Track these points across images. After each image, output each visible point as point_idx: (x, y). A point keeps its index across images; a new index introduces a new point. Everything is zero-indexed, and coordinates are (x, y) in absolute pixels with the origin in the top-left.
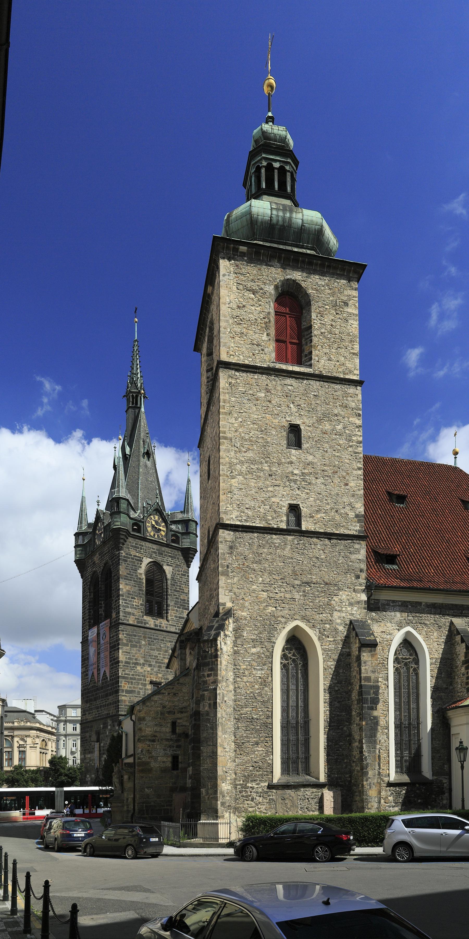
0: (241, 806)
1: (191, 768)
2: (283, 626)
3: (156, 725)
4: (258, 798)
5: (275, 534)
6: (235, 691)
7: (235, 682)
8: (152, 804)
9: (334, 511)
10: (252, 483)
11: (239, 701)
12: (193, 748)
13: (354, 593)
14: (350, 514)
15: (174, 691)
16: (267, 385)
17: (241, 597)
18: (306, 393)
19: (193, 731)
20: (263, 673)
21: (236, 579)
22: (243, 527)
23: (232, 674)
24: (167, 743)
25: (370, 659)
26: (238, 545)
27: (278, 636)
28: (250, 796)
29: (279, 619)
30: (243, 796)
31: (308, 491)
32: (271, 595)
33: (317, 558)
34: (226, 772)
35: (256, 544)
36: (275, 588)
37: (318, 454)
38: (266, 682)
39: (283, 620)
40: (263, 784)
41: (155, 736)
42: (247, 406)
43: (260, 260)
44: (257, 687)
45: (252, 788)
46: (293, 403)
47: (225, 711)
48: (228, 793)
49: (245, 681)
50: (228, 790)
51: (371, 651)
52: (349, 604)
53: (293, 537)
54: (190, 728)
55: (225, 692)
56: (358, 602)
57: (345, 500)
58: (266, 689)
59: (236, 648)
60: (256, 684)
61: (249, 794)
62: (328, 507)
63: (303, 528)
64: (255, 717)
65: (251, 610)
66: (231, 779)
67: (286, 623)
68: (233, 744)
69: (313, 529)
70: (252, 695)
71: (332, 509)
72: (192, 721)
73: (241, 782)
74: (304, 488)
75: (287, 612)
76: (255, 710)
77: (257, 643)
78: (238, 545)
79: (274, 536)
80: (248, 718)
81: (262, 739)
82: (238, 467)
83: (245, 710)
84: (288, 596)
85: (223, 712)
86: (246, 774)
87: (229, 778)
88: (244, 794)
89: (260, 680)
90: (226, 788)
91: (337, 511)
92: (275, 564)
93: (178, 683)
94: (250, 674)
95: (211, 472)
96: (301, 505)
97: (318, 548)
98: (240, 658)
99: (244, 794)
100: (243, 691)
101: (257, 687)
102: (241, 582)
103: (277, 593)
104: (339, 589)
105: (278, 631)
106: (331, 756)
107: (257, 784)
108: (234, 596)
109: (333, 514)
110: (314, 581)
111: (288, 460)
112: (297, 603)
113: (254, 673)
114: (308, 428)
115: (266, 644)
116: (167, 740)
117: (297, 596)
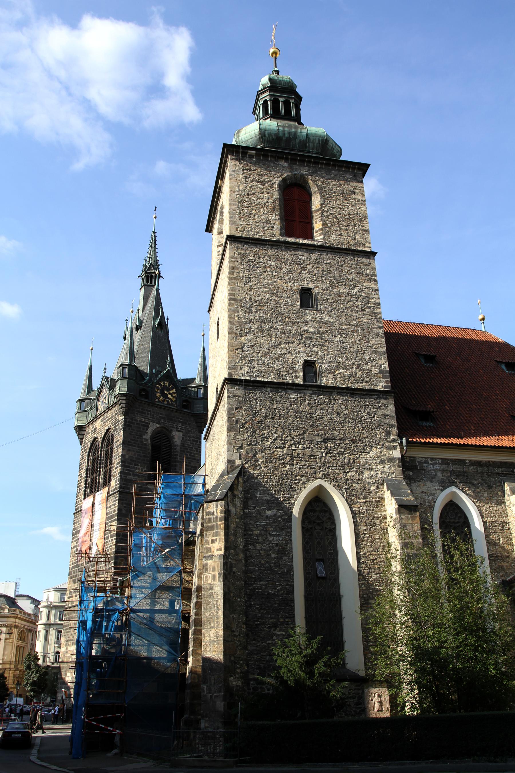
6: (246, 561)
7: (246, 550)
11: (251, 573)
20: (281, 539)
23: (242, 540)
25: (410, 522)
31: (326, 348)
34: (235, 663)
38: (285, 550)
43: (268, 160)
44: (273, 555)
47: (233, 584)
49: (258, 548)
50: (237, 686)
58: (284, 558)
60: (273, 553)
66: (241, 673)
68: (244, 626)
76: (272, 584)
77: (273, 505)
83: (259, 584)
84: (308, 452)
86: (262, 665)
89: (277, 548)
90: (234, 683)
94: (264, 540)
98: (253, 522)
105: (298, 491)
114: (321, 291)
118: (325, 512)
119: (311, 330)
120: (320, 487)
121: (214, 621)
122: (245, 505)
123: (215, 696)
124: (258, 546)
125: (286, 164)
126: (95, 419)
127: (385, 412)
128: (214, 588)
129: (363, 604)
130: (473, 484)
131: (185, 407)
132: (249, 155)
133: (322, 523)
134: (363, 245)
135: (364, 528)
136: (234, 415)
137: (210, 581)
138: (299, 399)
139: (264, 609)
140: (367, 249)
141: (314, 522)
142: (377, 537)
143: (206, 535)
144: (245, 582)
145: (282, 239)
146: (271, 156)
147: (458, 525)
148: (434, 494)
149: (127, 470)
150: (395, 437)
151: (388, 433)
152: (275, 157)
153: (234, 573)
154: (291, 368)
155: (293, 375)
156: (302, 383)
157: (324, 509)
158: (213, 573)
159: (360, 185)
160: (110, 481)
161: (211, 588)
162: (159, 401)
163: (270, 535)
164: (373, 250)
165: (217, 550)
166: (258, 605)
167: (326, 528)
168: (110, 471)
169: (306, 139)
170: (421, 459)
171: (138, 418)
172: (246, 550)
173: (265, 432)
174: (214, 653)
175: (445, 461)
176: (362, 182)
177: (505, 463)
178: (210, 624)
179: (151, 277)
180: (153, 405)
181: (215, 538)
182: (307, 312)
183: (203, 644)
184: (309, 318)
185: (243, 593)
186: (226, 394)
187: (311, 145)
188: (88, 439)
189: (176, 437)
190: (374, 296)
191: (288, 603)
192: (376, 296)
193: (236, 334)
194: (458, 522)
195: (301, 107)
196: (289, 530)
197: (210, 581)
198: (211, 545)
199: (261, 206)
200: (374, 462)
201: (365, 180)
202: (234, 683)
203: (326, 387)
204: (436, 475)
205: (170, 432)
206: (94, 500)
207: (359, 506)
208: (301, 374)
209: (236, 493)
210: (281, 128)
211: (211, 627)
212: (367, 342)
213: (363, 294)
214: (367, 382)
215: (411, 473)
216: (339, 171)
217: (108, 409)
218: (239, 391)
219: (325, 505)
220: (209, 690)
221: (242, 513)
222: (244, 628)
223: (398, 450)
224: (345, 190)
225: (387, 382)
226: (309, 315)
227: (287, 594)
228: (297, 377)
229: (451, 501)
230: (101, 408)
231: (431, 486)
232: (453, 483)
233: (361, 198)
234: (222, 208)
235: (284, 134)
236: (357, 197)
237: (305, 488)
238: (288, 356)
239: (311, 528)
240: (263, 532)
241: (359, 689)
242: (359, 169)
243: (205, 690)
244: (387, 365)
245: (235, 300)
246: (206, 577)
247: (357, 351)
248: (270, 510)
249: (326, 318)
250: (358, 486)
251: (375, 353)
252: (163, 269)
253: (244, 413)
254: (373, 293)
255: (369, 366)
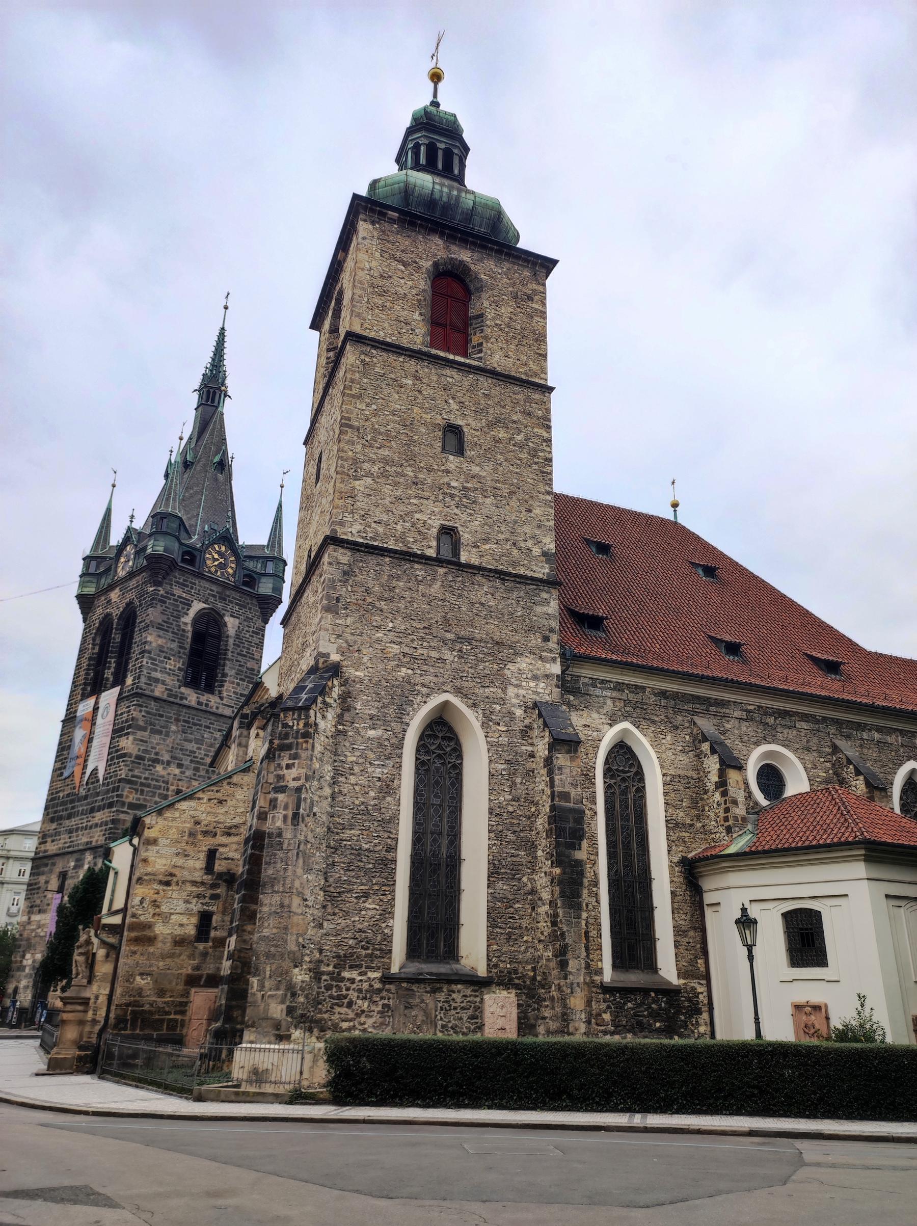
0: (326, 1016)
1: (233, 939)
2: (424, 699)
3: (177, 854)
4: (360, 1002)
5: (418, 563)
6: (333, 799)
7: (334, 783)
8: (146, 1007)
9: (509, 543)
10: (387, 490)
11: (339, 816)
12: (243, 900)
13: (540, 662)
14: (534, 549)
15: (219, 795)
16: (417, 371)
17: (356, 648)
18: (472, 389)
19: (247, 867)
20: (386, 771)
21: (349, 621)
22: (367, 546)
23: (330, 768)
24: (194, 889)
26: (357, 570)
27: (414, 715)
28: (345, 997)
29: (417, 688)
30: (331, 997)
32: (406, 650)
33: (481, 604)
34: (304, 947)
35: (387, 573)
36: (413, 641)
37: (488, 467)
38: (388, 788)
39: (425, 690)
40: (372, 975)
41: (172, 875)
42: (385, 392)
44: (372, 794)
45: (352, 981)
46: (453, 398)
47: (312, 831)
48: (302, 989)
49: (352, 782)
50: (303, 982)
51: (569, 752)
52: (533, 676)
53: (446, 570)
54: (241, 863)
55: (316, 798)
56: (547, 676)
57: (527, 531)
58: (389, 799)
59: (341, 727)
61: (344, 992)
62: (502, 537)
63: (463, 559)
64: (367, 846)
65: (371, 670)
66: (310, 962)
67: (428, 695)
68: (322, 893)
69: (477, 563)
70: (363, 807)
71: (507, 540)
72: (246, 850)
73: (331, 968)
74: (466, 507)
75: (431, 678)
77: (378, 722)
78: (357, 570)
79: (417, 566)
80: (352, 849)
81: (376, 887)
82: (366, 466)
84: (434, 654)
85: (309, 833)
86: (342, 953)
87: (307, 959)
88: (334, 992)
89: (379, 784)
90: (300, 977)
91: (514, 544)
92: (415, 605)
93: (229, 783)
95: (322, 472)
96: (460, 529)
97: (484, 592)
98: (347, 744)
99: (334, 992)
100: (348, 800)
101: (372, 794)
102: (358, 625)
103: (415, 648)
104: (515, 653)
105: (415, 706)
106: (500, 928)
107: (361, 974)
108: (344, 645)
109: (509, 547)
110: (478, 636)
111: (443, 468)
112: (448, 667)
113: (370, 770)
115: (393, 724)
116: (194, 883)
117: (448, 656)
118: (450, 739)
119: (454, 484)
120: (446, 704)
121: (279, 882)
122: (340, 719)
123: (270, 996)
124: (353, 779)
125: (440, 242)
126: (111, 588)
127: (545, 609)
128: (284, 834)
129: (492, 873)
130: (654, 722)
131: (245, 584)
132: (389, 218)
133: (445, 754)
134: (536, 375)
135: (503, 767)
136: (335, 589)
137: (279, 823)
138: (429, 578)
139: (353, 870)
140: (541, 382)
141: (434, 753)
142: (518, 780)
143: (279, 756)
144: (329, 829)
145: (426, 349)
146: (421, 226)
147: (628, 774)
148: (598, 730)
149: (152, 664)
150: (555, 646)
151: (546, 639)
152: (425, 228)
153: (315, 814)
154: (420, 533)
155: (423, 544)
156: (434, 556)
157: (448, 735)
158: (284, 812)
159: (541, 288)
160: (125, 676)
161: (280, 835)
162: (210, 572)
163: (370, 763)
164: (550, 384)
165: (294, 779)
166: (344, 863)
167: (449, 763)
168: (127, 664)
169: (472, 211)
170: (587, 680)
171: (178, 591)
172: (334, 783)
173: (377, 618)
174: (275, 931)
175: (619, 687)
176: (544, 285)
177: (698, 698)
178: (273, 886)
179: (212, 391)
180: (200, 576)
181: (292, 761)
182: (451, 458)
183: (258, 916)
184: (452, 467)
185: (324, 845)
186: (326, 559)
187: (477, 219)
188: (98, 613)
189: (229, 625)
190: (545, 448)
191: (387, 865)
192: (548, 449)
193: (348, 475)
194: (628, 772)
195: (468, 162)
196: (398, 760)
197: (279, 823)
198: (286, 771)
199: (398, 297)
200: (524, 676)
201: (548, 282)
202: (300, 977)
203: (469, 566)
204: (605, 703)
205: (222, 617)
206: (97, 703)
207: (497, 735)
208: (434, 543)
209: (328, 700)
210: (437, 187)
211: (274, 891)
212: (530, 511)
213: (530, 444)
214: (523, 565)
215: (572, 698)
216: (514, 264)
217: (131, 575)
218: (344, 556)
219: (451, 729)
220: (262, 987)
221: (333, 729)
222: (321, 896)
223: (559, 663)
224: (519, 293)
225: (551, 568)
226: (453, 461)
227: (386, 851)
228: (429, 547)
229: (622, 741)
230: (121, 573)
231: (595, 718)
232: (626, 717)
233: (540, 308)
234: (341, 293)
235: (441, 197)
236: (535, 306)
237: (425, 702)
238: (417, 516)
239: (429, 760)
240: (361, 760)
241: (477, 996)
242: (542, 265)
243: (255, 985)
244: (553, 546)
245: (351, 427)
246: (273, 817)
247: (516, 522)
248: (374, 729)
249: (476, 470)
250: (498, 707)
251: (539, 527)
252: (231, 383)
253: (349, 588)
254: (545, 444)
255: (530, 543)
